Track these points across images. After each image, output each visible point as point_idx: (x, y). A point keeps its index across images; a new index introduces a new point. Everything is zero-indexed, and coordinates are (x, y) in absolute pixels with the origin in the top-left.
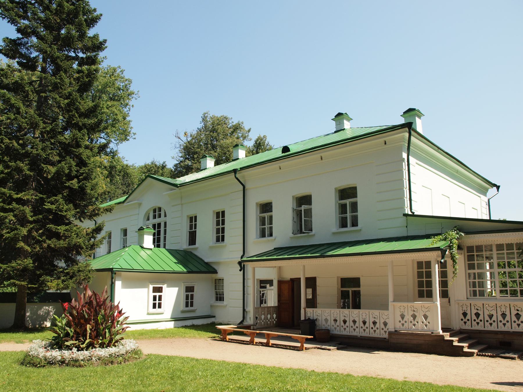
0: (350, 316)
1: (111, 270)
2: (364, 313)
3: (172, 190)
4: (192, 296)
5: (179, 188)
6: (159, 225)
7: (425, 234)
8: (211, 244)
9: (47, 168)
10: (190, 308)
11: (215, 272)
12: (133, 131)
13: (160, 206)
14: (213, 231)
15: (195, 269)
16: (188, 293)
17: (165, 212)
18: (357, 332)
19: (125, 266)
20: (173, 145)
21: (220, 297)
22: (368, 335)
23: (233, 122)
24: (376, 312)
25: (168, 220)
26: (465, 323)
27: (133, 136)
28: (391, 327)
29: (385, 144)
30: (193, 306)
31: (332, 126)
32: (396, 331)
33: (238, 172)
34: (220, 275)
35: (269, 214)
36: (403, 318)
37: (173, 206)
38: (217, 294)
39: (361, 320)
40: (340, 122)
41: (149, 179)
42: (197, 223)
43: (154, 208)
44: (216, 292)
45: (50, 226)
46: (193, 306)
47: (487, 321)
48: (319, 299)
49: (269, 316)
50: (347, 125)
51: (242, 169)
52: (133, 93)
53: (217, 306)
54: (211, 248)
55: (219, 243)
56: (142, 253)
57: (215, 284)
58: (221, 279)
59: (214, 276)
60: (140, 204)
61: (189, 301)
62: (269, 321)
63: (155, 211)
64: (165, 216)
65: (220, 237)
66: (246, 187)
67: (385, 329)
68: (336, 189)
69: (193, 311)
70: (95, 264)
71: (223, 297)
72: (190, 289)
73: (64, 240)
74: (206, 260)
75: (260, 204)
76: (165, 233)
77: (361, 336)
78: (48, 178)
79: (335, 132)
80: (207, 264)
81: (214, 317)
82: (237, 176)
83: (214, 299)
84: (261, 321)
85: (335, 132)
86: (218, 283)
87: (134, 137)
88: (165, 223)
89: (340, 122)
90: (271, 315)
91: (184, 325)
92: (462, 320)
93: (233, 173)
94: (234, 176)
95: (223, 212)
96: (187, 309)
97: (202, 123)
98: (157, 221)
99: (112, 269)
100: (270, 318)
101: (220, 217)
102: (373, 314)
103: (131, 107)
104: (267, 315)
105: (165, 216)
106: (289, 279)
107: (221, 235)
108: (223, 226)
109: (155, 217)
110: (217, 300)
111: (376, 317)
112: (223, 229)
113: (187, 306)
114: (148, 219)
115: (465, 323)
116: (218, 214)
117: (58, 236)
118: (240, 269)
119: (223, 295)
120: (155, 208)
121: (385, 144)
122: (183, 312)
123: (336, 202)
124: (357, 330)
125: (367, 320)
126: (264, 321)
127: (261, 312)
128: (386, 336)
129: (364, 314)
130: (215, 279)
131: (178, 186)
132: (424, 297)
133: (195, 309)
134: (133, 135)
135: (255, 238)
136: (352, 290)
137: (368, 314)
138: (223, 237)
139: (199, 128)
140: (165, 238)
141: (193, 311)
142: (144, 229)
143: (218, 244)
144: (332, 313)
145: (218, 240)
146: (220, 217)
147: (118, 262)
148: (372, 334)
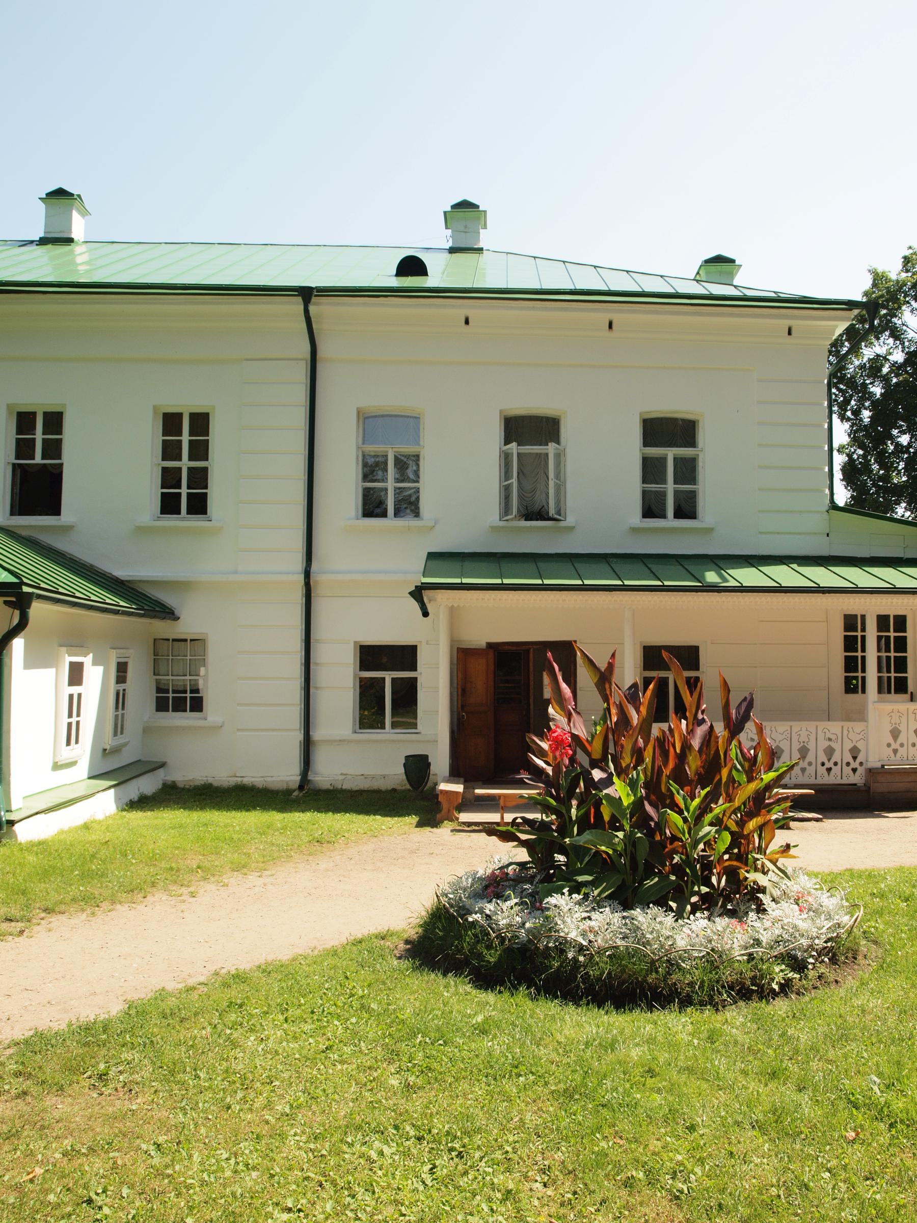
2: (804, 729)
11: (167, 613)
18: (810, 776)
24: (835, 727)
29: (790, 333)
33: (314, 299)
38: (159, 690)
39: (796, 746)
40: (466, 227)
54: (142, 531)
55: (177, 519)
58: (186, 640)
59: (161, 628)
66: (320, 354)
81: (162, 765)
82: (311, 308)
89: (466, 227)
91: (135, 796)
93: (300, 299)
94: (302, 307)
95: (201, 422)
102: (825, 730)
106: (484, 645)
111: (833, 737)
116: (171, 422)
118: (420, 613)
121: (790, 333)
124: (836, 770)
135: (353, 513)
137: (814, 732)
143: (171, 521)
145: (169, 505)
148: (822, 776)
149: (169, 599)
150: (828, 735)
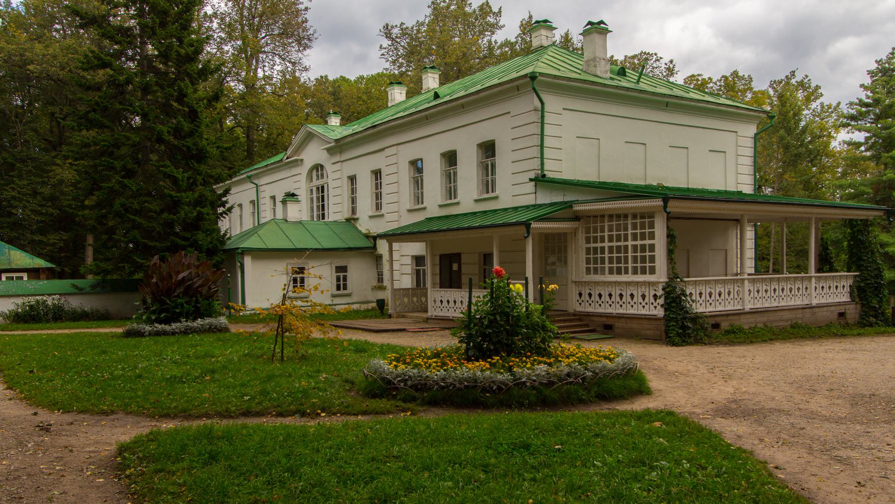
6: (323, 187)
8: (370, 214)
10: (342, 292)
14: (372, 196)
16: (338, 274)
37: (333, 164)
38: (379, 275)
54: (371, 217)
69: (349, 295)
72: (342, 269)
98: (320, 182)
100: (417, 301)
104: (412, 298)
109: (318, 179)
113: (338, 288)
114: (311, 181)
122: (334, 296)
132: (646, 274)
141: (349, 295)
145: (377, 209)
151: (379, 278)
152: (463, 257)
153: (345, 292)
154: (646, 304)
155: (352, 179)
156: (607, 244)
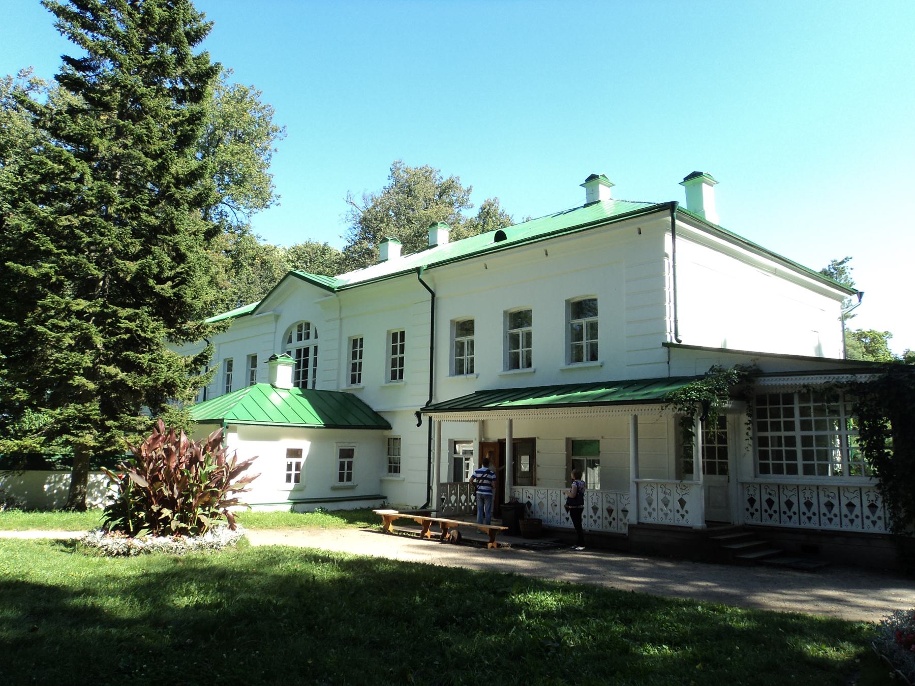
0: (536, 496)
1: (220, 422)
3: (327, 296)
4: (350, 464)
5: (337, 293)
6: (307, 350)
7: (694, 375)
8: (383, 384)
9: (125, 265)
10: (345, 483)
11: (388, 427)
12: (275, 192)
13: (309, 321)
15: (354, 422)
16: (342, 460)
17: (316, 331)
19: (243, 416)
20: (344, 217)
21: (394, 468)
22: (615, 530)
23: (441, 178)
25: (320, 343)
26: (752, 514)
27: (276, 200)
28: (632, 518)
30: (350, 480)
31: (581, 197)
32: (639, 523)
34: (396, 431)
35: (469, 338)
36: (650, 504)
38: (390, 462)
41: (291, 277)
42: (364, 349)
43: (298, 324)
44: (389, 458)
45: (128, 353)
46: (350, 480)
47: (785, 513)
48: (540, 472)
49: (463, 498)
50: (604, 192)
51: (430, 266)
52: (276, 130)
53: (390, 480)
54: (383, 387)
55: (395, 382)
56: (274, 396)
57: (389, 445)
60: (277, 317)
61: (346, 471)
62: (463, 505)
63: (300, 327)
64: (316, 337)
65: (397, 374)
66: (437, 295)
67: (625, 521)
68: (567, 302)
69: (352, 488)
70: (199, 412)
71: (399, 466)
73: (149, 375)
74: (375, 409)
75: (458, 323)
76: (315, 364)
77: (590, 531)
78: (127, 282)
79: (585, 206)
80: (376, 414)
81: (385, 498)
83: (386, 469)
84: (450, 505)
85: (585, 206)
86: (393, 444)
87: (277, 202)
88: (316, 348)
90: (466, 495)
92: (748, 510)
95: (403, 334)
96: (342, 484)
97: (392, 180)
98: (303, 344)
99: (223, 420)
100: (466, 501)
101: (398, 340)
103: (273, 154)
104: (461, 495)
105: (316, 337)
107: (398, 368)
108: (394, 356)
110: (390, 471)
112: (402, 359)
113: (341, 479)
114: (290, 341)
115: (752, 514)
116: (395, 335)
117: (140, 370)
118: (418, 423)
119: (400, 464)
120: (301, 323)
122: (334, 489)
123: (505, 332)
125: (599, 506)
126: (455, 505)
127: (451, 491)
128: (625, 530)
129: (554, 495)
130: (389, 439)
131: (336, 289)
133: (355, 484)
134: (275, 198)
135: (448, 374)
136: (589, 459)
138: (401, 372)
139: (387, 187)
140: (315, 371)
142: (277, 358)
144: (589, 495)
145: (394, 377)
146: (398, 340)
147: (232, 410)
149: (387, 418)
150: (528, 495)
151: (390, 467)
152: (539, 445)
153: (349, 483)
154: (814, 514)
155: (357, 344)
156: (798, 433)
